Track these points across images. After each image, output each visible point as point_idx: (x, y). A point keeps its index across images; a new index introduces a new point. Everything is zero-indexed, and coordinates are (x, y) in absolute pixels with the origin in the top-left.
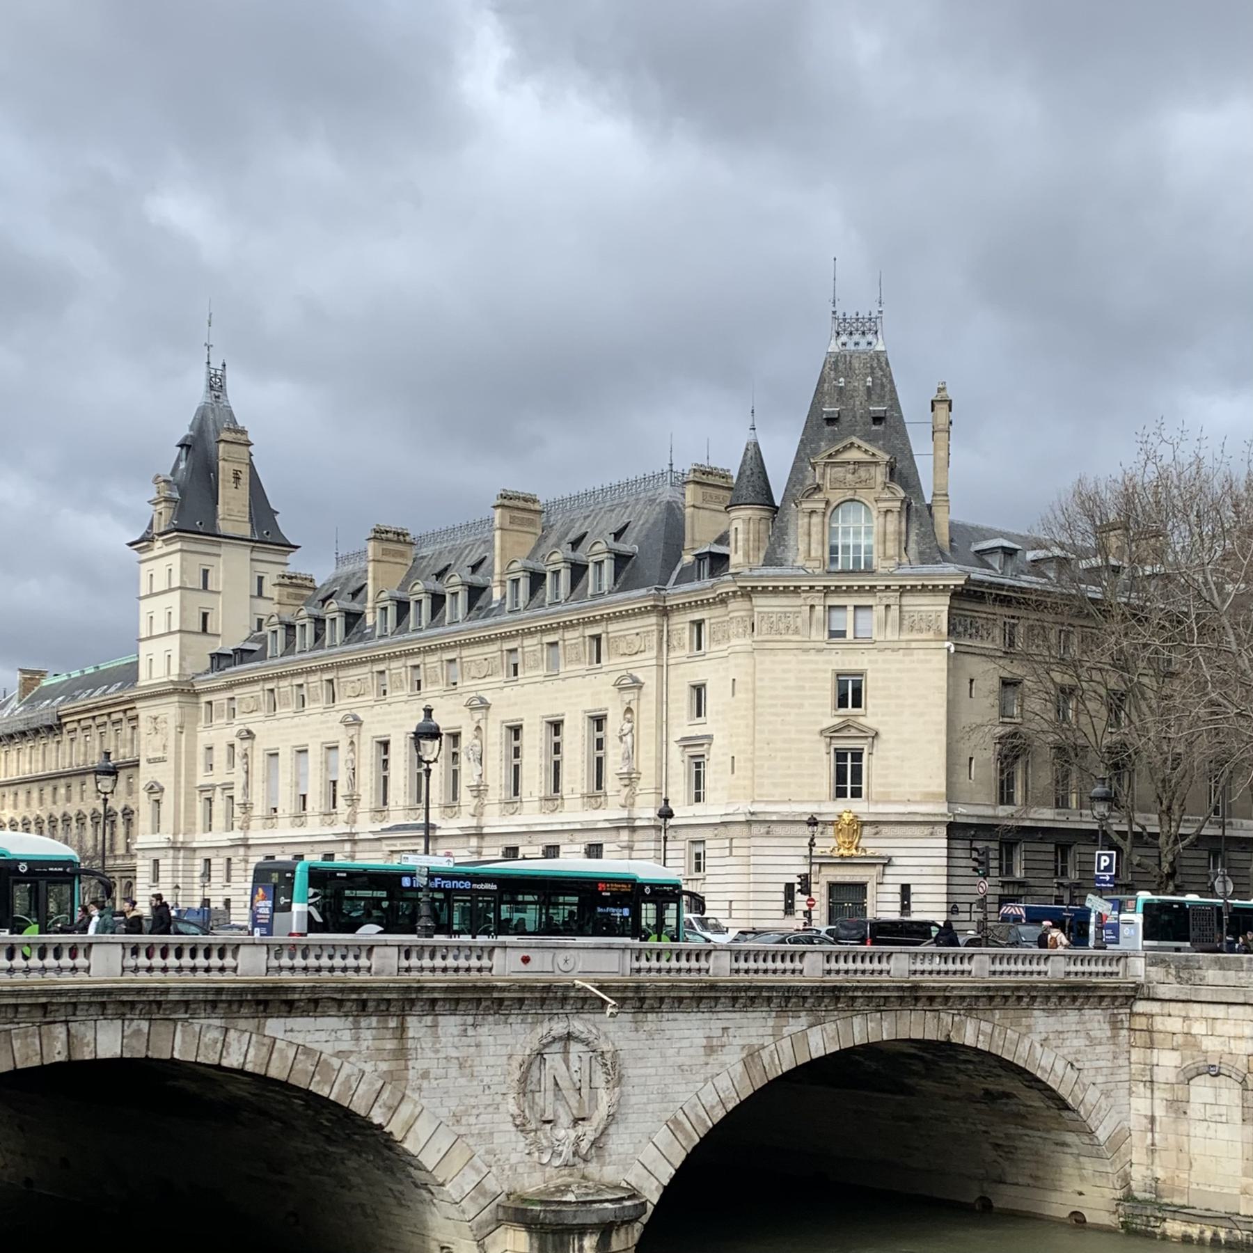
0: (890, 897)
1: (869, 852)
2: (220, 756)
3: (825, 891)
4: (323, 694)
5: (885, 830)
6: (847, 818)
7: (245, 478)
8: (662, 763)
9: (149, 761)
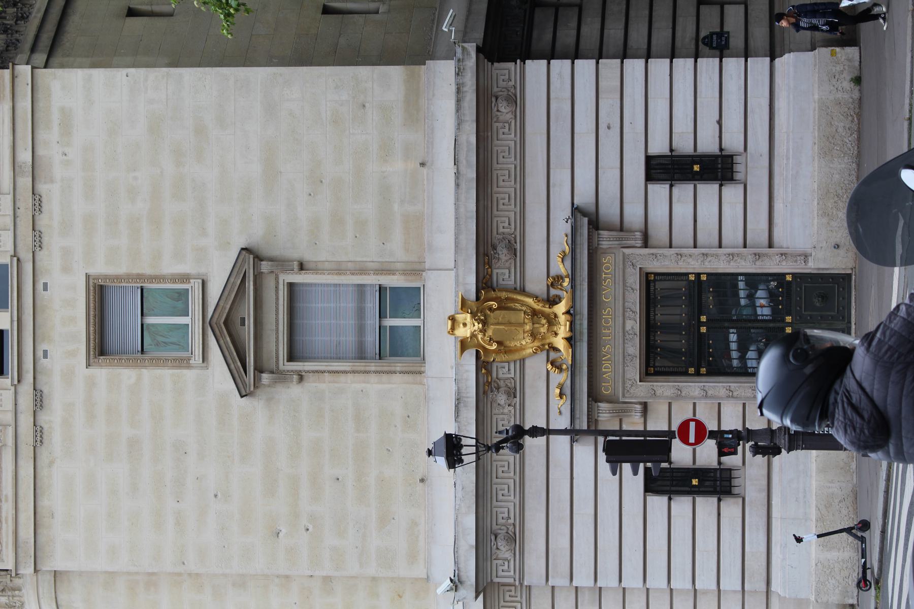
0: (683, 210)
1: (560, 268)
3: (665, 387)
5: (503, 223)
6: (468, 328)
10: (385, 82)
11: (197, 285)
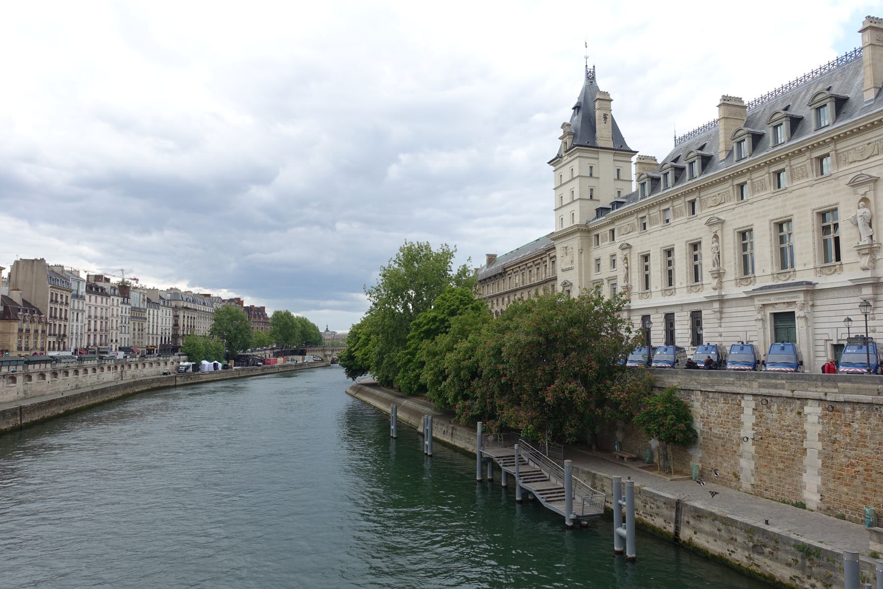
2: (605, 263)
4: (686, 211)
9: (563, 270)
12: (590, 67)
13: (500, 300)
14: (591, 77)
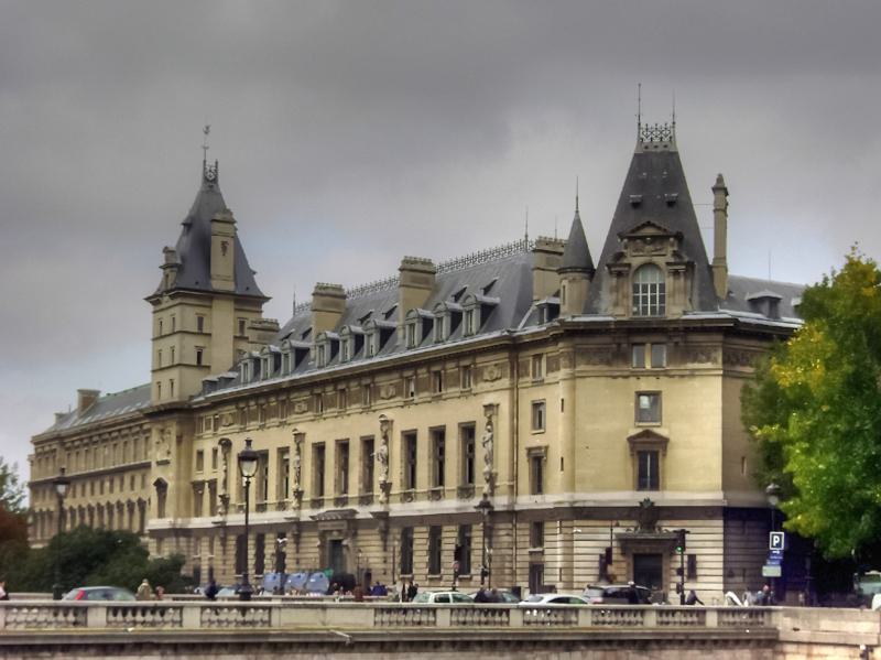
7: (231, 249)
8: (514, 465)
10: (718, 480)
11: (658, 424)
12: (211, 163)
13: (97, 484)
14: (211, 182)
